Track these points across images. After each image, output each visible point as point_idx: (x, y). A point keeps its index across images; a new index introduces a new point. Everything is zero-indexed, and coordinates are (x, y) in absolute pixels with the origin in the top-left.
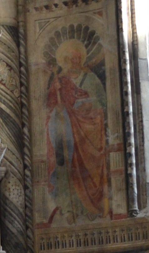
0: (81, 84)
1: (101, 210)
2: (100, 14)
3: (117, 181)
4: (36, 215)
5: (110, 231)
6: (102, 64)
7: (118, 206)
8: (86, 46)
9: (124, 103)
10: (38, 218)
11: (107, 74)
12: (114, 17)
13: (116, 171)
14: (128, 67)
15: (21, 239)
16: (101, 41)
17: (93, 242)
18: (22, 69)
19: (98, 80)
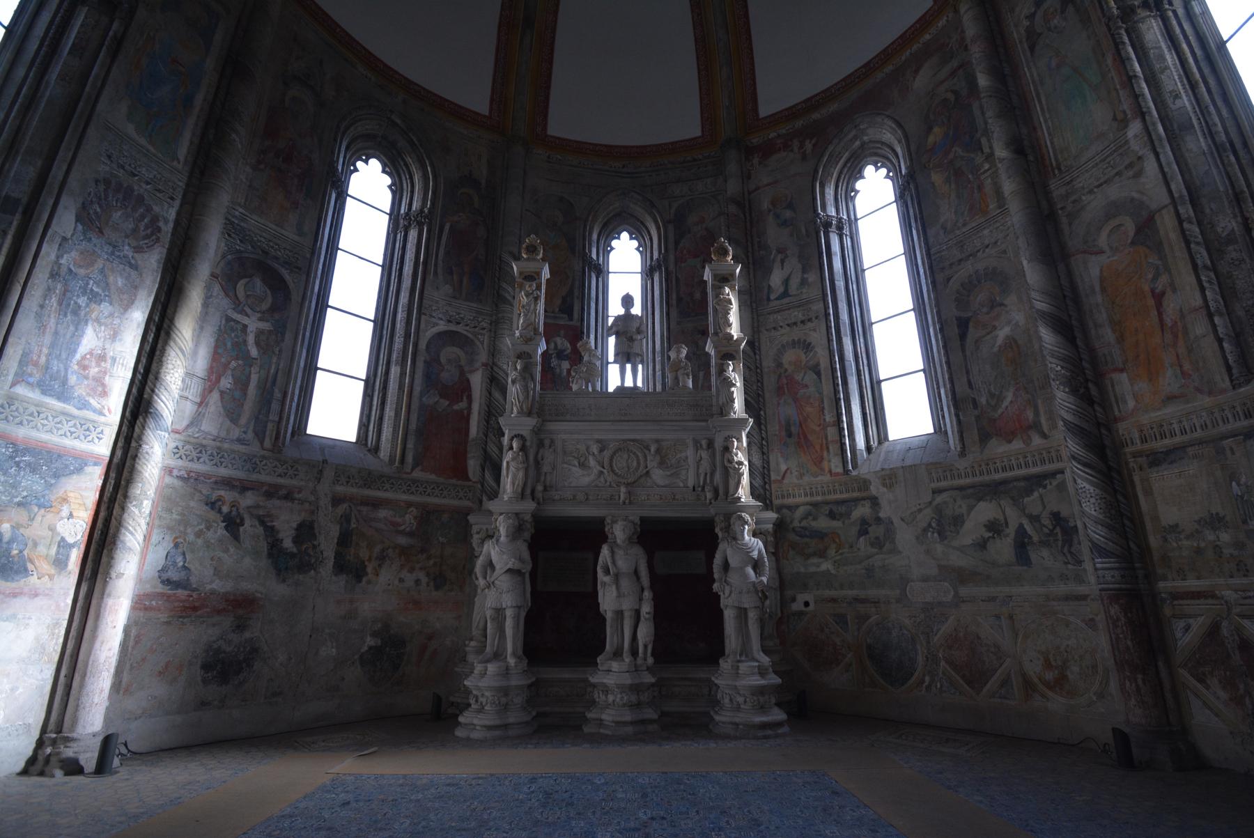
0: (802, 380)
1: (822, 469)
2: (815, 330)
3: (834, 448)
4: (772, 473)
5: (807, 488)
6: (818, 364)
7: (836, 466)
8: (805, 353)
9: (836, 392)
10: (773, 477)
11: (822, 372)
12: (825, 332)
13: (833, 441)
14: (838, 366)
15: (762, 491)
16: (816, 349)
17: (818, 494)
18: (758, 370)
19: (815, 377)
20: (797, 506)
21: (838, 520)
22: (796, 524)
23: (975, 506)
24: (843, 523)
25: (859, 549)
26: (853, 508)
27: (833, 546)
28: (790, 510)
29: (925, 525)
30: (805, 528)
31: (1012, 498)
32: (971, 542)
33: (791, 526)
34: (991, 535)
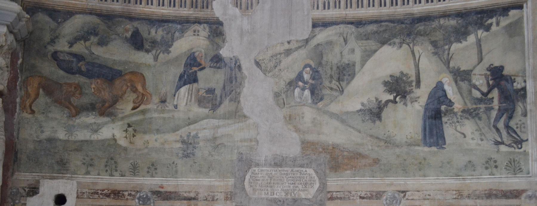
20: (70, 14)
21: (148, 51)
22: (62, 46)
23: (375, 51)
24: (156, 58)
25: (176, 107)
26: (177, 34)
27: (131, 97)
28: (54, 19)
29: (292, 76)
30: (80, 58)
31: (434, 44)
32: (359, 107)
33: (51, 49)
34: (391, 97)
